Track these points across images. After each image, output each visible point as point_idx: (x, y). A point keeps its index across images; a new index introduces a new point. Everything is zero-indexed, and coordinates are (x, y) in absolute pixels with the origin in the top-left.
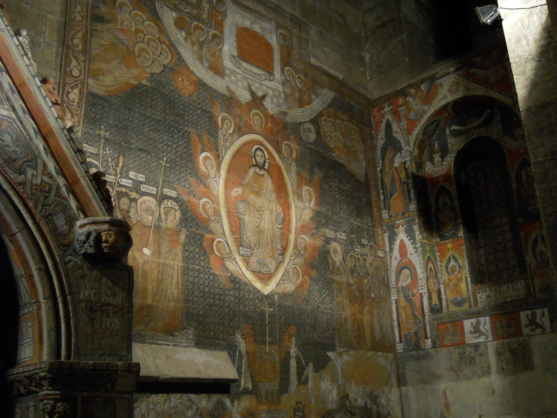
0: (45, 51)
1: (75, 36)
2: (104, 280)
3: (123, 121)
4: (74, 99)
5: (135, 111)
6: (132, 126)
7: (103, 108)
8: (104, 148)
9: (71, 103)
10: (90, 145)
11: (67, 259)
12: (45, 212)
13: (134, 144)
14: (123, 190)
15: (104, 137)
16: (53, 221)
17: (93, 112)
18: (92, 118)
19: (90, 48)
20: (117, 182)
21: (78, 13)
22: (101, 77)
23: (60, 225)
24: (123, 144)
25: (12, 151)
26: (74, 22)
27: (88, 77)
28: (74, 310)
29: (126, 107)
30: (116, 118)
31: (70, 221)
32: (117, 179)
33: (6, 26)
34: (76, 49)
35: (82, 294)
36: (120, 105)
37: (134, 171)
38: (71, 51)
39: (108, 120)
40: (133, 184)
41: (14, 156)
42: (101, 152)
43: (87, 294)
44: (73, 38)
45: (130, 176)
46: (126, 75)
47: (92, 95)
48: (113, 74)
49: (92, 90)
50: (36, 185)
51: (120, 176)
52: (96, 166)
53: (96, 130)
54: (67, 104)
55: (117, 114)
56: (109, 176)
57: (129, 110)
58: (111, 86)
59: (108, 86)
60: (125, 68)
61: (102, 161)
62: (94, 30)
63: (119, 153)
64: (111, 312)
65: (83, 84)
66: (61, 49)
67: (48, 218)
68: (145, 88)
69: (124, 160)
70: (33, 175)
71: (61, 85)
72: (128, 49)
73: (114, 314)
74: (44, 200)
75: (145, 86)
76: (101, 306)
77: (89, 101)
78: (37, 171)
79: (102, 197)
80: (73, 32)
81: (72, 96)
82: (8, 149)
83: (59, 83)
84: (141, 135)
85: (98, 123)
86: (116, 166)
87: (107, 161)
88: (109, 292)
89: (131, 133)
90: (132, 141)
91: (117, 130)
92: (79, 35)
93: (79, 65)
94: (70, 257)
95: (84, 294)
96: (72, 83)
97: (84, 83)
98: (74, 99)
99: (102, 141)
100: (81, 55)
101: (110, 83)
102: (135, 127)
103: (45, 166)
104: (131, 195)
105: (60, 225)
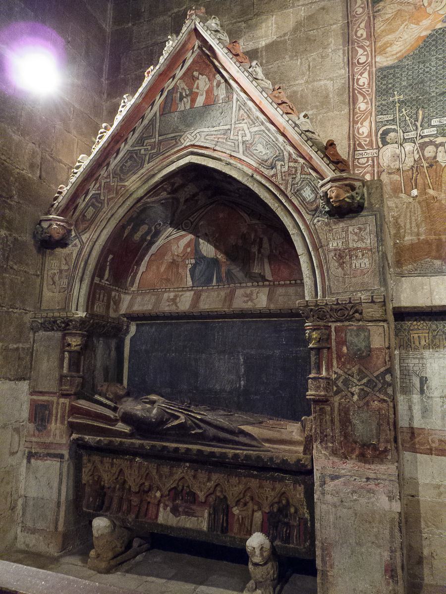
0: (333, 58)
1: (358, 29)
2: (351, 229)
3: (418, 76)
4: (364, 83)
5: (430, 60)
6: (429, 76)
7: (394, 76)
8: (399, 111)
9: (361, 87)
10: (386, 115)
11: (315, 221)
12: (294, 190)
13: (433, 92)
14: (427, 140)
15: (399, 101)
16: (301, 194)
17: (384, 85)
18: (384, 90)
19: (374, 30)
20: (418, 135)
21: (359, 7)
22: (389, 49)
23: (307, 196)
24: (420, 98)
25: (264, 155)
26: (356, 17)
27: (375, 56)
28: (325, 258)
29: (419, 62)
30: (410, 78)
31: (315, 189)
32: (419, 133)
33: (239, 67)
34: (360, 39)
35: (331, 245)
36: (413, 63)
37: (437, 118)
38: (356, 44)
39: (401, 84)
40: (437, 130)
41: (265, 158)
42: (398, 115)
43: (335, 245)
44: (356, 31)
45: (432, 124)
46: (416, 32)
47: (381, 69)
48: (401, 39)
49: (381, 65)
50: (284, 172)
51: (421, 128)
52: (394, 130)
53: (389, 99)
54: (358, 91)
55: (410, 73)
56: (409, 133)
57: (424, 62)
58: (401, 51)
59: (396, 54)
60: (414, 26)
61: (400, 123)
62: (376, 12)
63: (417, 108)
64: (360, 254)
65: (371, 66)
66: (346, 48)
67: (297, 193)
68: (440, 32)
69: (423, 112)
70: (282, 165)
71: (351, 77)
72: (415, 5)
73: (363, 255)
74: (292, 182)
75: (440, 29)
76: (349, 251)
77: (378, 77)
78: (284, 161)
79: (328, 162)
80: (355, 27)
81: (361, 83)
82: (261, 154)
83: (349, 76)
84: (441, 79)
85: (391, 91)
86: (415, 121)
87: (405, 120)
88: (356, 238)
89: (428, 83)
90: (432, 90)
91: (413, 87)
92: (363, 25)
93: (365, 50)
94: (318, 218)
95: (333, 245)
96: (360, 70)
97: (372, 63)
98: (364, 83)
99: (398, 105)
100: (366, 41)
101: (398, 49)
102: (433, 75)
103: (290, 154)
104: (436, 141)
105: (307, 196)
